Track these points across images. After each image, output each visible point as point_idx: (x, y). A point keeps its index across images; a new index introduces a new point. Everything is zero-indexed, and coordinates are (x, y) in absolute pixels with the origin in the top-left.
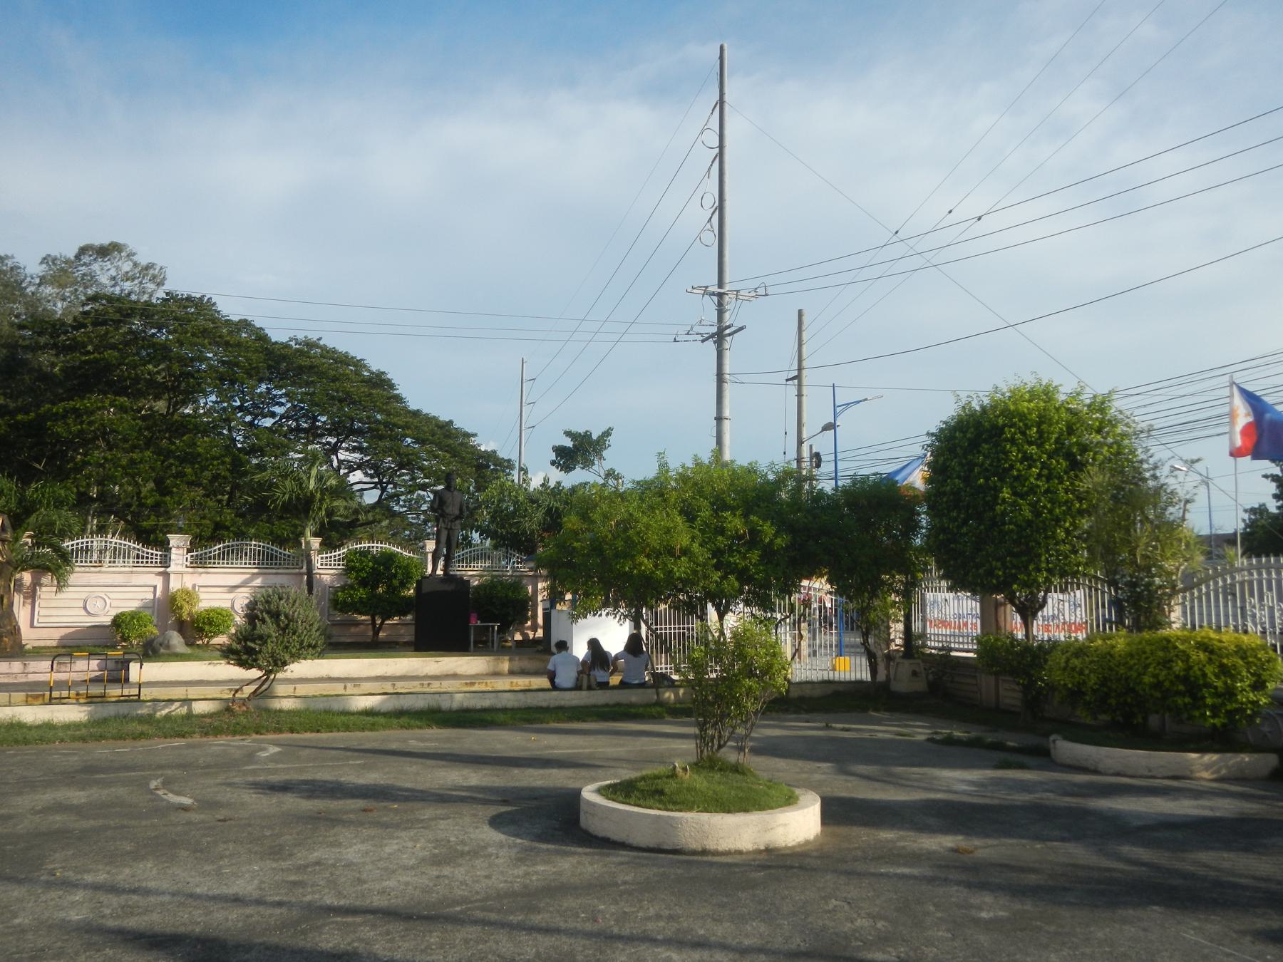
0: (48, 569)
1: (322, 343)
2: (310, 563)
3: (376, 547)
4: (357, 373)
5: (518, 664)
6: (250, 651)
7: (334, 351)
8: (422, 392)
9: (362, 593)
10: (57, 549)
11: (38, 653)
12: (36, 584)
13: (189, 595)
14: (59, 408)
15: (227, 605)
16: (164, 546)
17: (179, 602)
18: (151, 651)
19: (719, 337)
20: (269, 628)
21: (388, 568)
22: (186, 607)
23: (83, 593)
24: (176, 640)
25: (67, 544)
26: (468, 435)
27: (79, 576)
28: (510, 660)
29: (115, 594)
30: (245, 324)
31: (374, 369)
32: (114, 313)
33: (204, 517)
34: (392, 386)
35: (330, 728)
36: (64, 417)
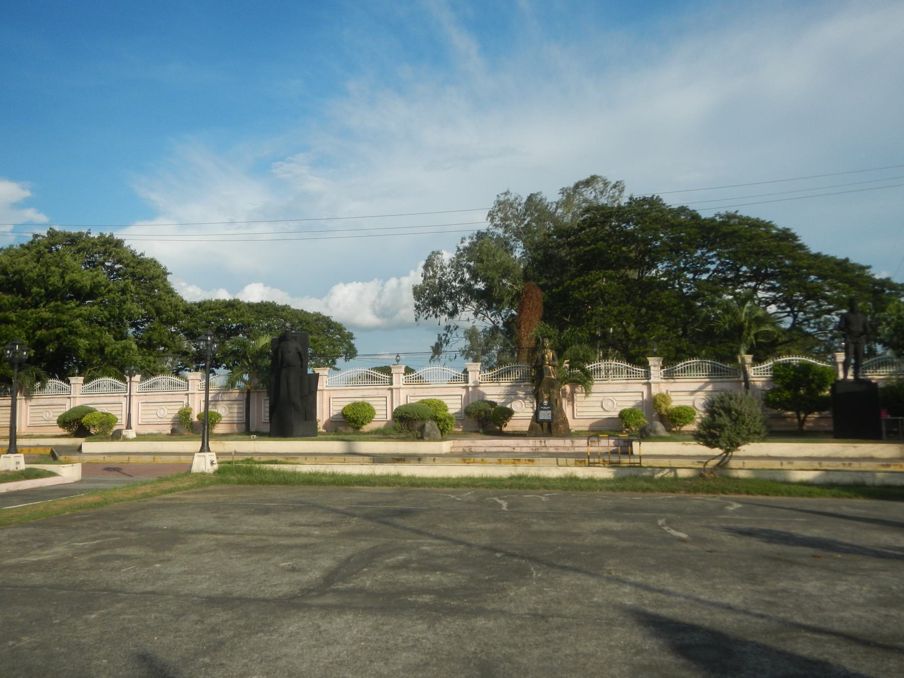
0: (578, 383)
1: (738, 214)
3: (795, 359)
4: (768, 232)
6: (713, 436)
7: (748, 219)
8: (820, 237)
10: (583, 370)
11: (579, 435)
12: (573, 392)
13: (665, 398)
15: (690, 404)
16: (645, 365)
17: (659, 402)
18: (645, 435)
20: (725, 420)
21: (807, 376)
22: (664, 406)
23: (600, 397)
24: (660, 428)
27: (597, 386)
30: (683, 209)
31: (780, 227)
32: (600, 216)
33: (669, 345)
34: (794, 237)
35: (777, 493)
36: (579, 287)
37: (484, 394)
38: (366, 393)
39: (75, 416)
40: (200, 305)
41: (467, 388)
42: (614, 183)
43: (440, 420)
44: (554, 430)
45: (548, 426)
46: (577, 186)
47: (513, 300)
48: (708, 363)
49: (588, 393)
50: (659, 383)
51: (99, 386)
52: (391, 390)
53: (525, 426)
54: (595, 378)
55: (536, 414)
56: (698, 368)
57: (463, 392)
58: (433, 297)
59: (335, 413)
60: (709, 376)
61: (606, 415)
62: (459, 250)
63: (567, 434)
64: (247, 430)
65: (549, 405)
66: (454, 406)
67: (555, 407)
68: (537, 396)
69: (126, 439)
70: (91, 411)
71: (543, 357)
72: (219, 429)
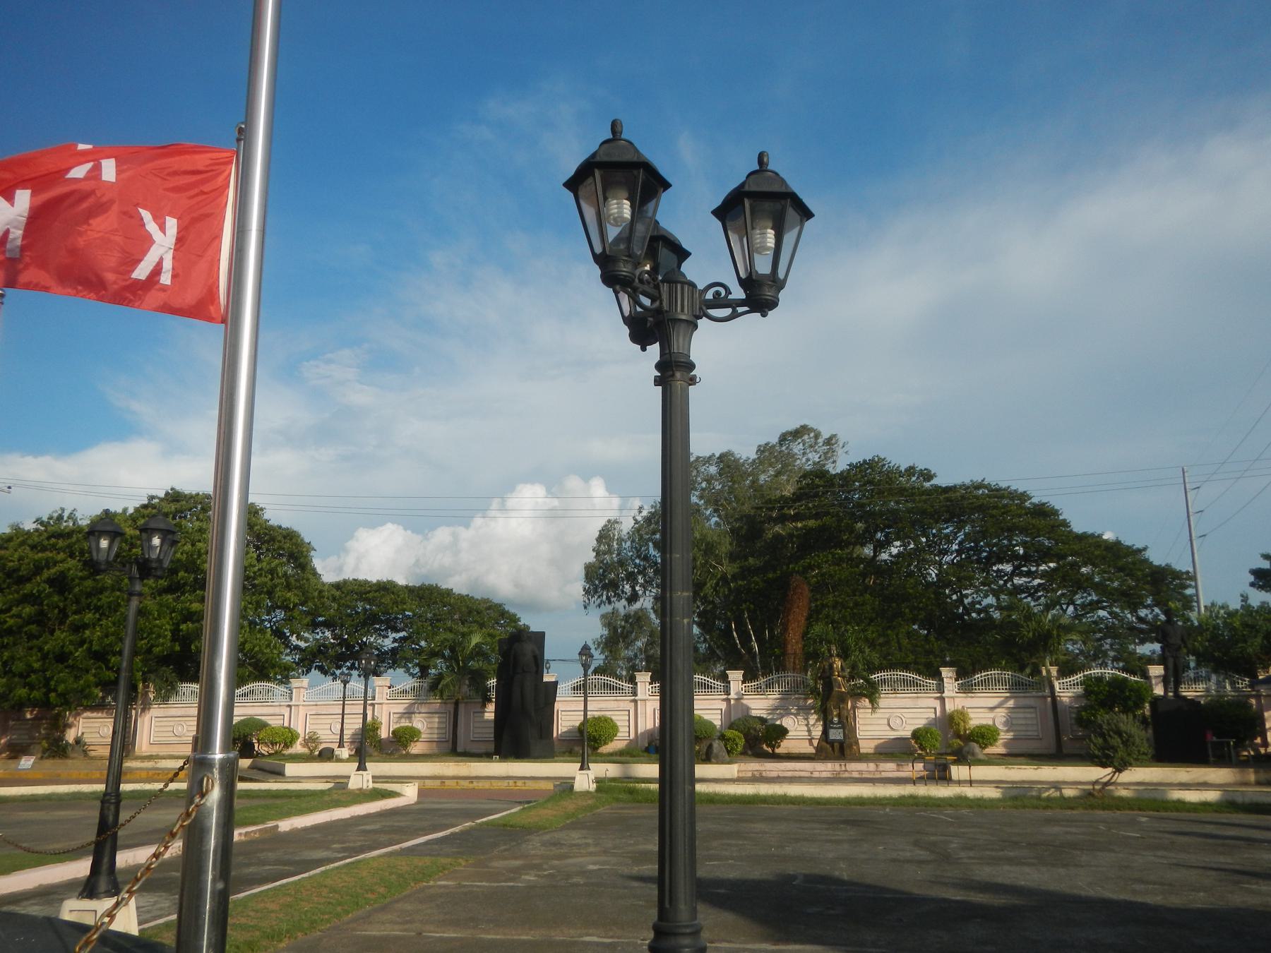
0: (861, 695)
2: (1052, 687)
4: (1020, 506)
5: (1263, 776)
6: (1108, 757)
8: (1083, 516)
10: (867, 680)
12: (854, 708)
13: (962, 714)
15: (990, 723)
16: (937, 675)
26: (1139, 551)
27: (886, 700)
28: (1256, 772)
29: (907, 714)
34: (1055, 513)
37: (748, 709)
38: (603, 705)
39: (247, 730)
40: (337, 586)
41: (728, 700)
42: (826, 435)
43: (728, 740)
44: (847, 752)
45: (838, 747)
46: (783, 438)
47: (717, 584)
48: (1008, 674)
49: (874, 707)
50: (955, 699)
51: (252, 692)
52: (635, 702)
54: (884, 689)
55: (825, 732)
56: (998, 681)
57: (723, 706)
58: (603, 578)
59: (565, 729)
60: (1010, 690)
64: (452, 748)
65: (840, 722)
67: (847, 724)
69: (339, 760)
70: (264, 725)
71: (831, 666)
72: (416, 749)
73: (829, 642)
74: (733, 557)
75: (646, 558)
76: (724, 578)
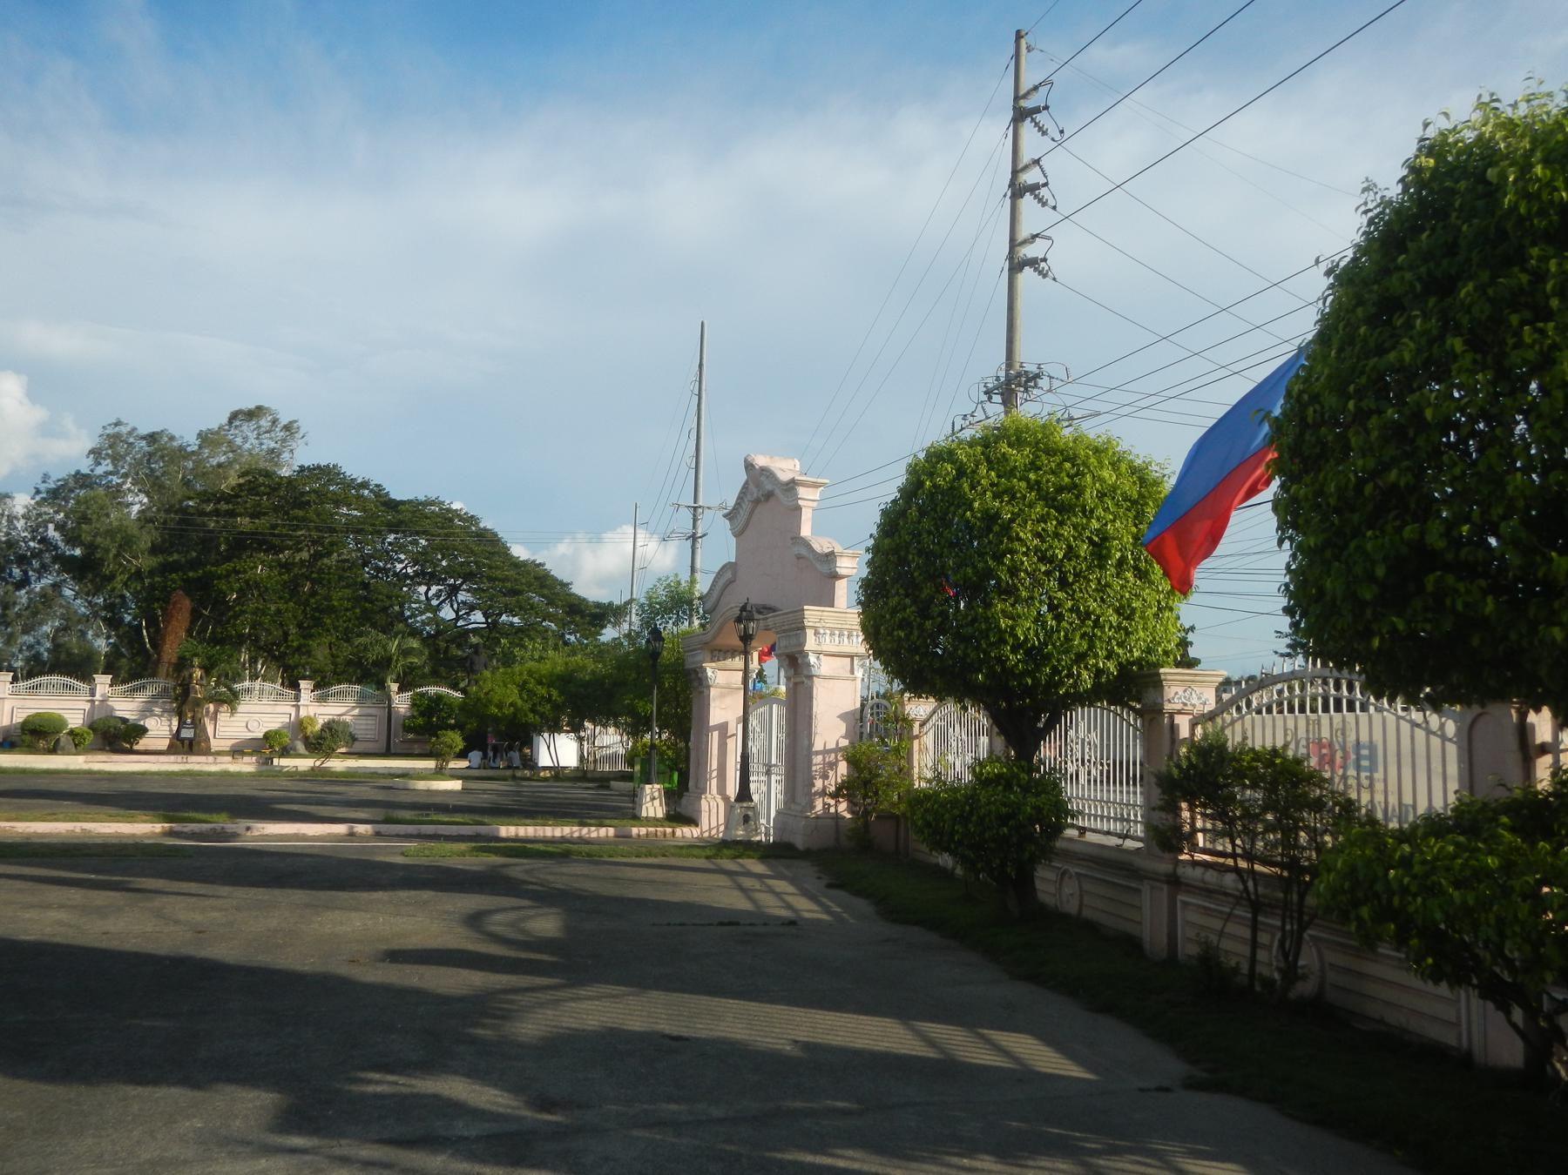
2: (390, 699)
3: (432, 690)
9: (420, 721)
10: (230, 689)
12: (216, 712)
13: (312, 720)
14: (222, 570)
16: (296, 687)
18: (286, 752)
19: (694, 538)
23: (245, 718)
25: (237, 686)
29: (265, 718)
36: (228, 576)
37: (113, 709)
44: (195, 748)
49: (233, 711)
53: (164, 744)
55: (178, 731)
57: (87, 706)
61: (250, 735)
62: (38, 492)
63: (207, 752)
66: (75, 720)
67: (197, 724)
68: (180, 715)
73: (196, 655)
74: (154, 550)
75: (44, 540)
76: (138, 575)
